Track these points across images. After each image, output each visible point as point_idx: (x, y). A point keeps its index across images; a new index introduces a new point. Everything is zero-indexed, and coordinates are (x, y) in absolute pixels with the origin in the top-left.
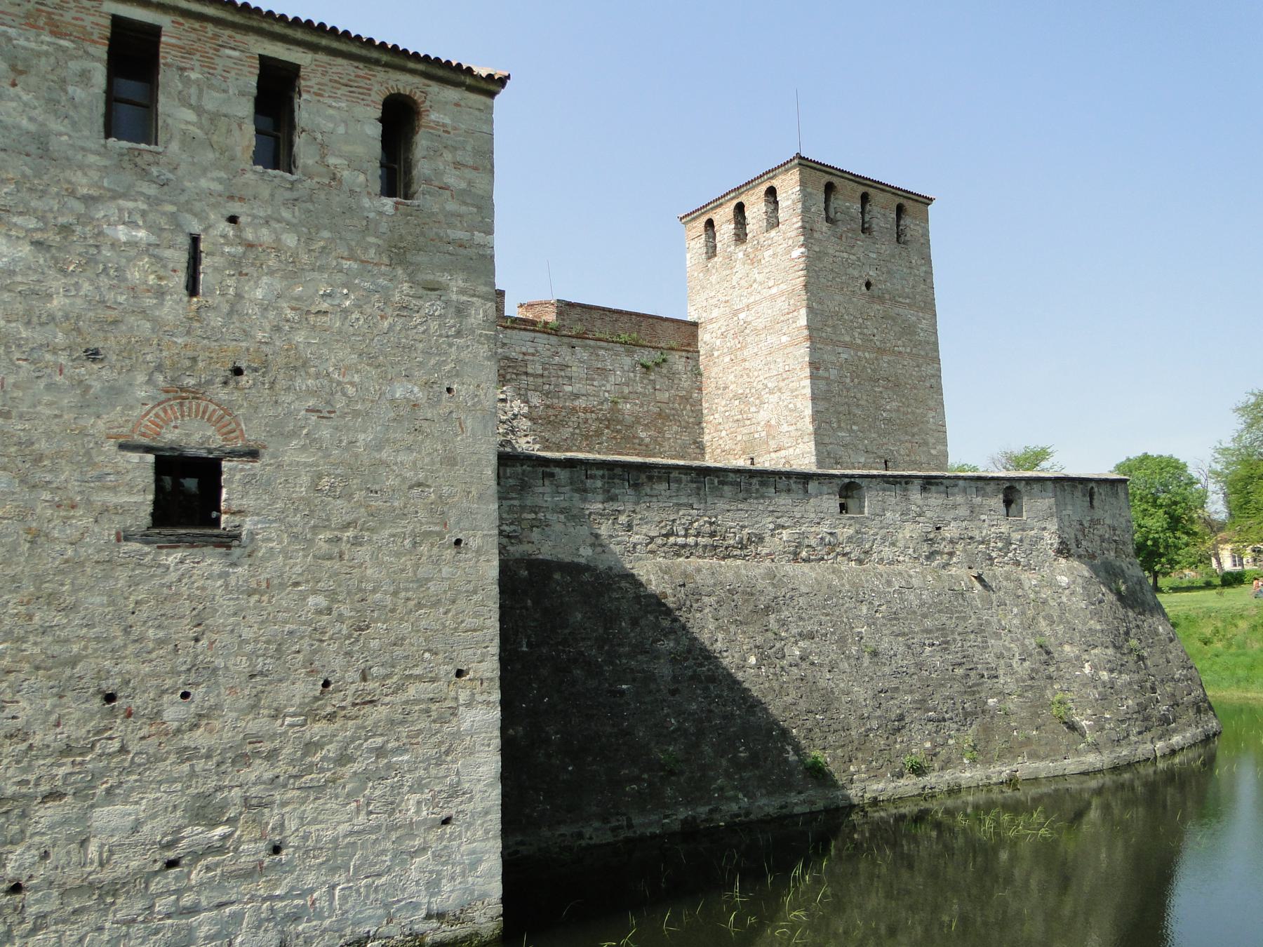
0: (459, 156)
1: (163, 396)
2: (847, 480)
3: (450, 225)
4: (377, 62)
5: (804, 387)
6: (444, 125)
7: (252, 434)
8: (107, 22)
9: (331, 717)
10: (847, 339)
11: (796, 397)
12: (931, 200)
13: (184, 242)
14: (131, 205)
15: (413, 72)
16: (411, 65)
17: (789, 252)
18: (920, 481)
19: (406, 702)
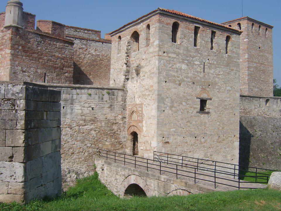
0: (236, 46)
1: (201, 90)
2: (267, 99)
3: (234, 59)
4: (226, 30)
5: (246, 72)
6: (234, 41)
7: (211, 96)
8: (194, 27)
9: (219, 142)
10: (255, 61)
11: (244, 74)
12: (273, 27)
13: (203, 64)
14: (197, 58)
15: (230, 32)
16: (230, 31)
17: (244, 40)
18: (280, 99)
19: (228, 140)
